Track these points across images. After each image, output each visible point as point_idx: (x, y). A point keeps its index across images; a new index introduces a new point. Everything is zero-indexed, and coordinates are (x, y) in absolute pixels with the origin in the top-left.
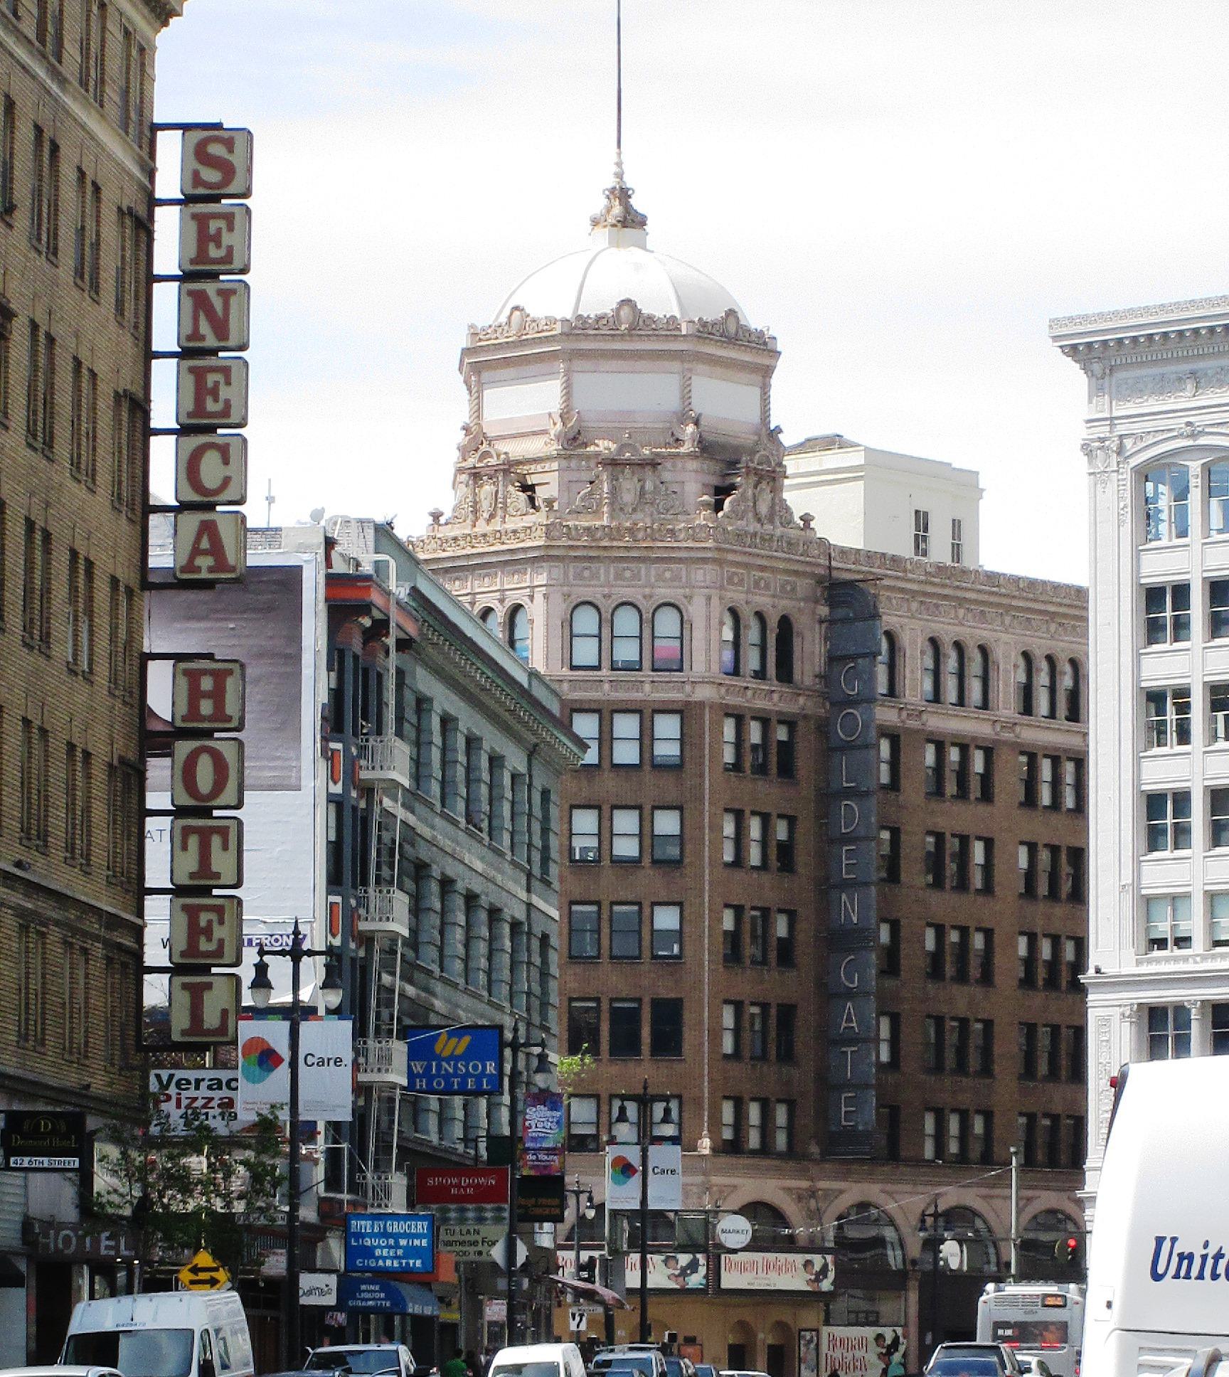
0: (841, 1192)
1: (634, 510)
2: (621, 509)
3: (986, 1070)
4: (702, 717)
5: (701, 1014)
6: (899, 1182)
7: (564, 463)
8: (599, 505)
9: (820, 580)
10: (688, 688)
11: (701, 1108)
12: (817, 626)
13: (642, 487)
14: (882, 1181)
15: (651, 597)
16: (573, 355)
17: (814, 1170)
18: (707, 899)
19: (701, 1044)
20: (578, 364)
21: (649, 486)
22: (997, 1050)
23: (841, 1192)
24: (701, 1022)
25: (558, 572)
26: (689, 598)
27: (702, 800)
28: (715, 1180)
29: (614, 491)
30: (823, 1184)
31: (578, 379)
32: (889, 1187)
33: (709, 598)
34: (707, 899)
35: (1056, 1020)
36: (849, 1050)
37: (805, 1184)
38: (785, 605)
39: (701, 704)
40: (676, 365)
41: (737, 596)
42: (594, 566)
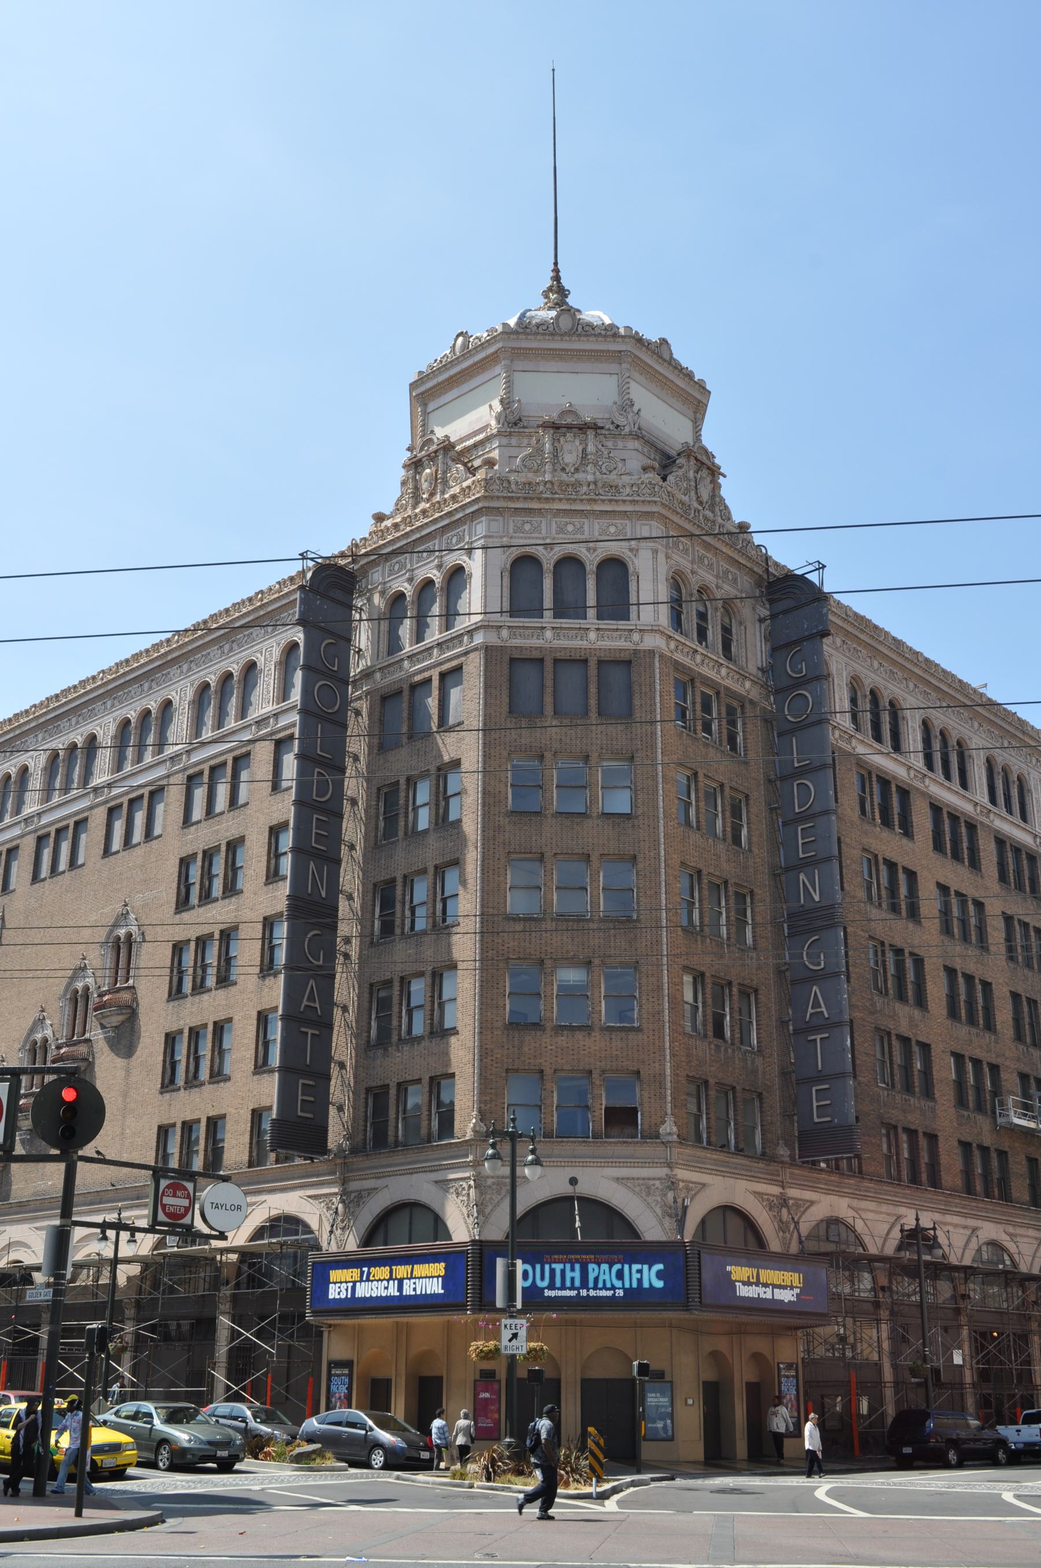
0: (812, 1203)
1: (577, 470)
2: (563, 469)
3: (928, 1093)
4: (652, 666)
5: (660, 979)
6: (865, 1198)
7: (505, 441)
8: (543, 464)
9: (759, 582)
10: (636, 637)
11: (662, 1085)
12: (757, 625)
13: (584, 450)
14: (852, 1196)
15: (595, 550)
16: (517, 354)
17: (787, 1174)
18: (662, 853)
19: (660, 1012)
20: (519, 365)
21: (591, 448)
22: (936, 1075)
23: (812, 1203)
24: (660, 988)
25: (497, 524)
26: (635, 551)
27: (653, 747)
28: (681, 1174)
29: (555, 454)
30: (793, 1193)
31: (518, 377)
32: (855, 1203)
33: (655, 552)
34: (662, 853)
35: (978, 1054)
36: (818, 1037)
37: (775, 1190)
38: (728, 590)
39: (651, 653)
40: (614, 367)
41: (685, 564)
42: (536, 520)
